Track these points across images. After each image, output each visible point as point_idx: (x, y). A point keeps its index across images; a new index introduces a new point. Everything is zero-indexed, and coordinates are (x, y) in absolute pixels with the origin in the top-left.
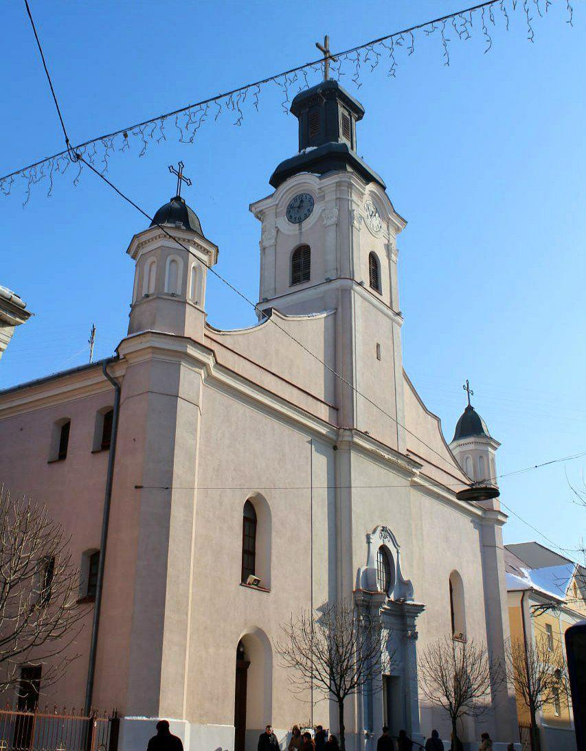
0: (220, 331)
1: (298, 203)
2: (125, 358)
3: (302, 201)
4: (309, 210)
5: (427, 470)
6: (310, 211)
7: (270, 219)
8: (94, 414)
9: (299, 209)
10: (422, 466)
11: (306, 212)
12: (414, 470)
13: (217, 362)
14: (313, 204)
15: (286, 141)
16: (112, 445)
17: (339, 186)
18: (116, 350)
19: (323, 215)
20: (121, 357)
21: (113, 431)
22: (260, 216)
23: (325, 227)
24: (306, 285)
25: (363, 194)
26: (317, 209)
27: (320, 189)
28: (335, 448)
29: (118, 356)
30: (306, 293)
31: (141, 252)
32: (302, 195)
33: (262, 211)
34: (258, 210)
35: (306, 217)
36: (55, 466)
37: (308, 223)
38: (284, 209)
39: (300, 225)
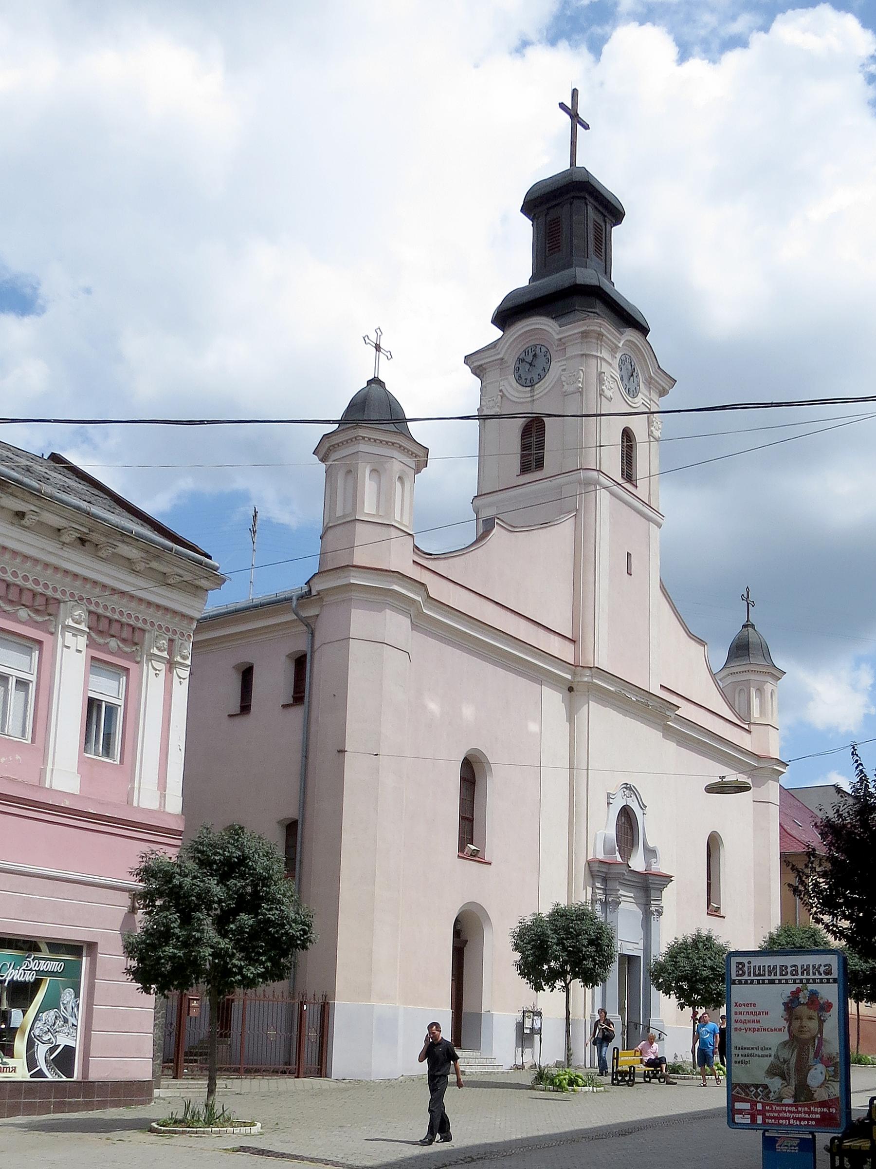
0: (431, 555)
1: (529, 359)
2: (319, 594)
3: (535, 356)
4: (544, 369)
5: (686, 711)
6: (545, 370)
7: (493, 375)
8: (283, 658)
9: (531, 366)
10: (678, 707)
11: (540, 371)
12: (668, 713)
13: (429, 596)
14: (549, 361)
15: (513, 264)
16: (306, 700)
17: (586, 337)
18: (308, 583)
19: (563, 378)
20: (314, 593)
21: (307, 680)
22: (478, 371)
23: (565, 395)
24: (538, 475)
25: (617, 347)
26: (555, 369)
27: (560, 339)
28: (571, 689)
29: (310, 590)
30: (537, 485)
31: (334, 456)
32: (535, 346)
33: (481, 365)
34: (475, 364)
35: (540, 380)
36: (237, 720)
37: (542, 388)
38: (511, 362)
39: (532, 391)
